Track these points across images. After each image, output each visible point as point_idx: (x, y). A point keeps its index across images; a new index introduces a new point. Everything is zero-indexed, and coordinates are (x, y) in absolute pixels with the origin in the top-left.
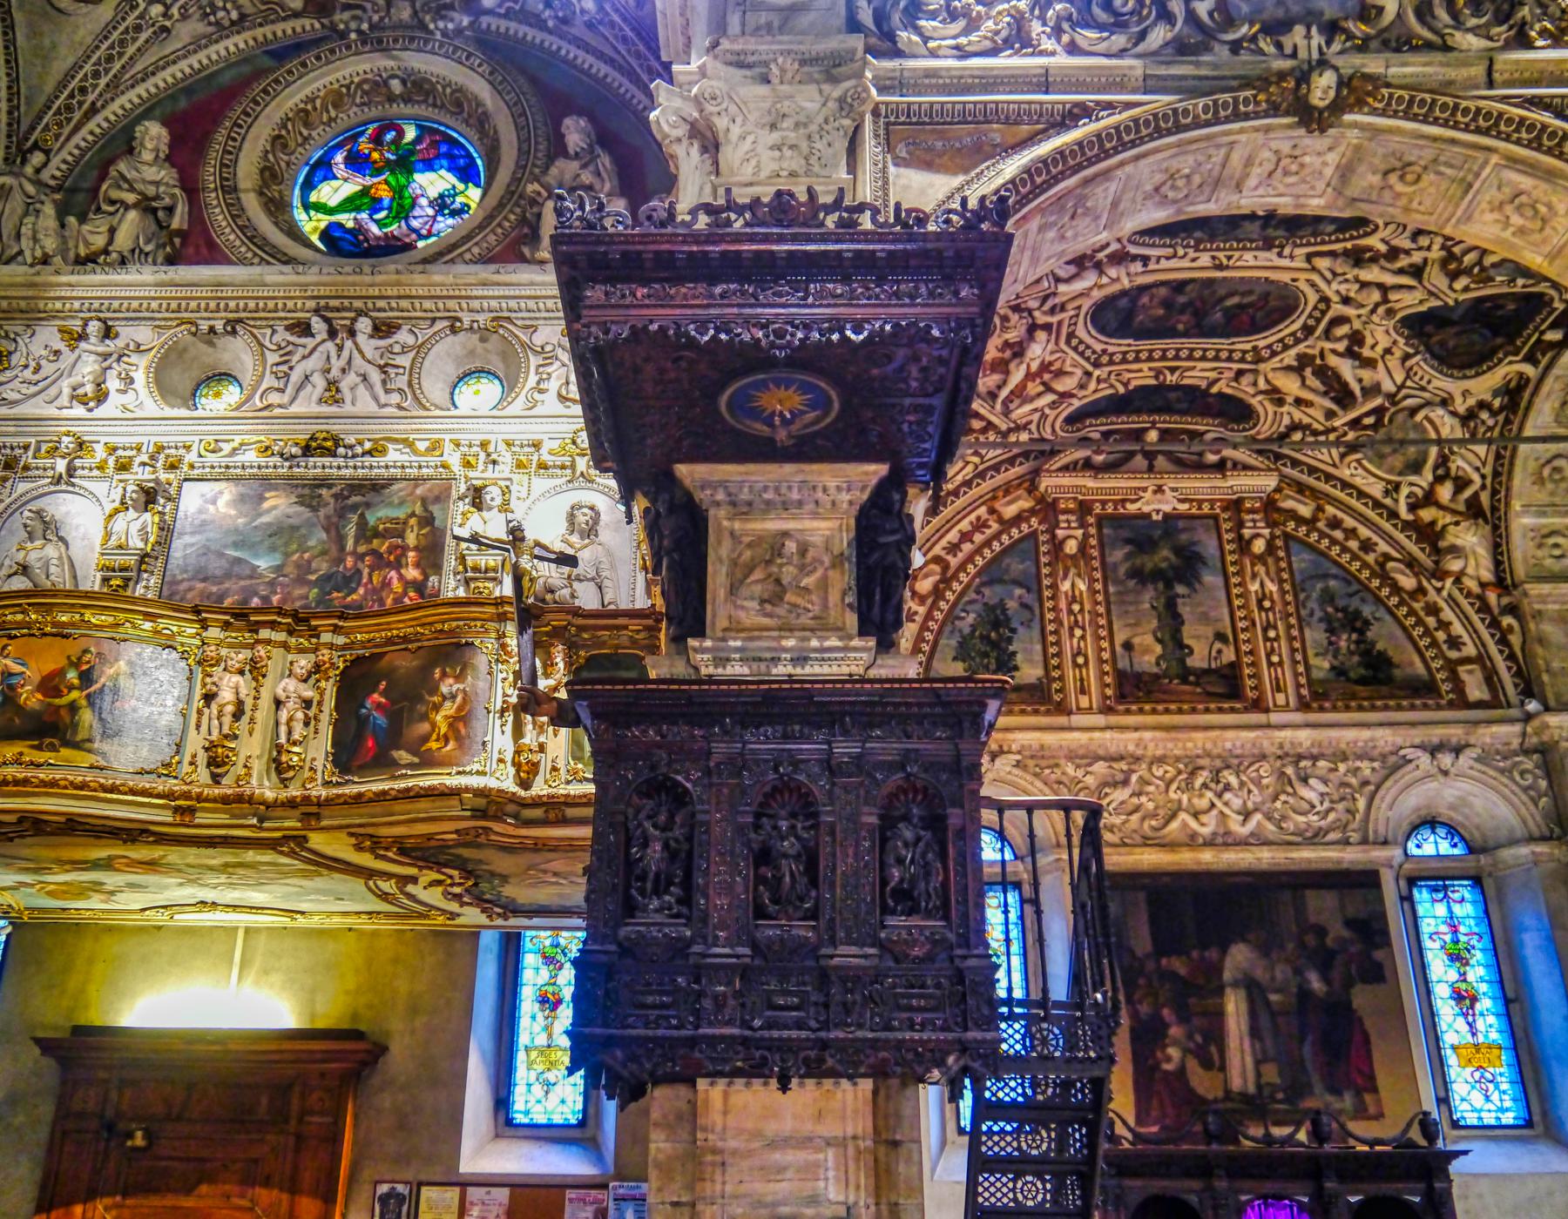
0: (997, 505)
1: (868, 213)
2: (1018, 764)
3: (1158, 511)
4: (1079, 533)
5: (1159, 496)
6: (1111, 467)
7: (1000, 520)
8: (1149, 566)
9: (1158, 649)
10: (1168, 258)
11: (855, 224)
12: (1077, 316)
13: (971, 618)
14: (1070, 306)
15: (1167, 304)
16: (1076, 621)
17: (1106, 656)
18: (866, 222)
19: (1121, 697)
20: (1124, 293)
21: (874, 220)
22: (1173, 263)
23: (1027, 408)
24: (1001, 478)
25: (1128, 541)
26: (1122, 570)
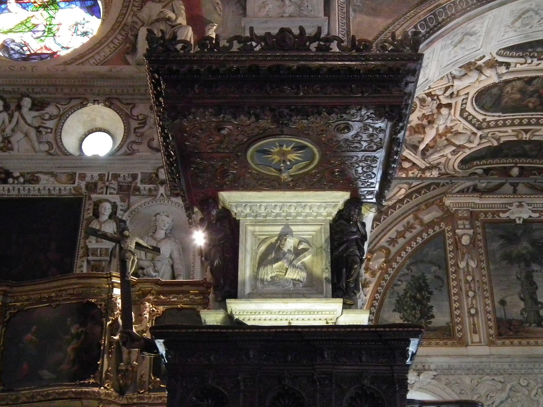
0: (420, 216)
1: (336, 42)
2: (435, 377)
3: (520, 218)
4: (472, 231)
5: (520, 209)
6: (491, 191)
7: (421, 223)
8: (516, 252)
9: (522, 304)
10: (521, 64)
11: (328, 49)
12: (467, 98)
13: (404, 286)
14: (462, 93)
15: (521, 91)
16: (470, 287)
17: (489, 309)
18: (334, 47)
19: (500, 335)
20: (495, 85)
21: (339, 46)
22: (525, 67)
23: (437, 156)
24: (421, 198)
25: (502, 237)
26: (498, 256)
